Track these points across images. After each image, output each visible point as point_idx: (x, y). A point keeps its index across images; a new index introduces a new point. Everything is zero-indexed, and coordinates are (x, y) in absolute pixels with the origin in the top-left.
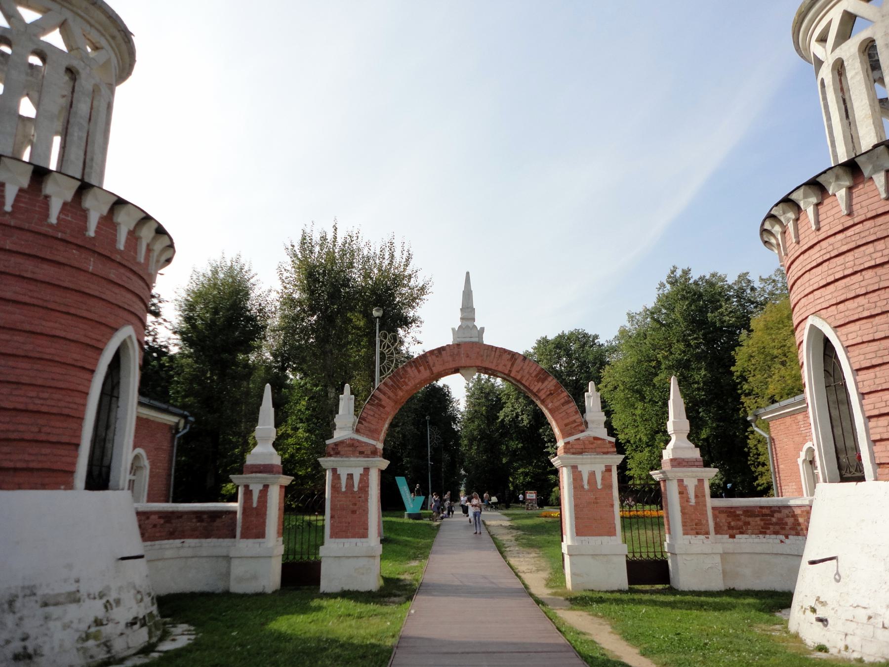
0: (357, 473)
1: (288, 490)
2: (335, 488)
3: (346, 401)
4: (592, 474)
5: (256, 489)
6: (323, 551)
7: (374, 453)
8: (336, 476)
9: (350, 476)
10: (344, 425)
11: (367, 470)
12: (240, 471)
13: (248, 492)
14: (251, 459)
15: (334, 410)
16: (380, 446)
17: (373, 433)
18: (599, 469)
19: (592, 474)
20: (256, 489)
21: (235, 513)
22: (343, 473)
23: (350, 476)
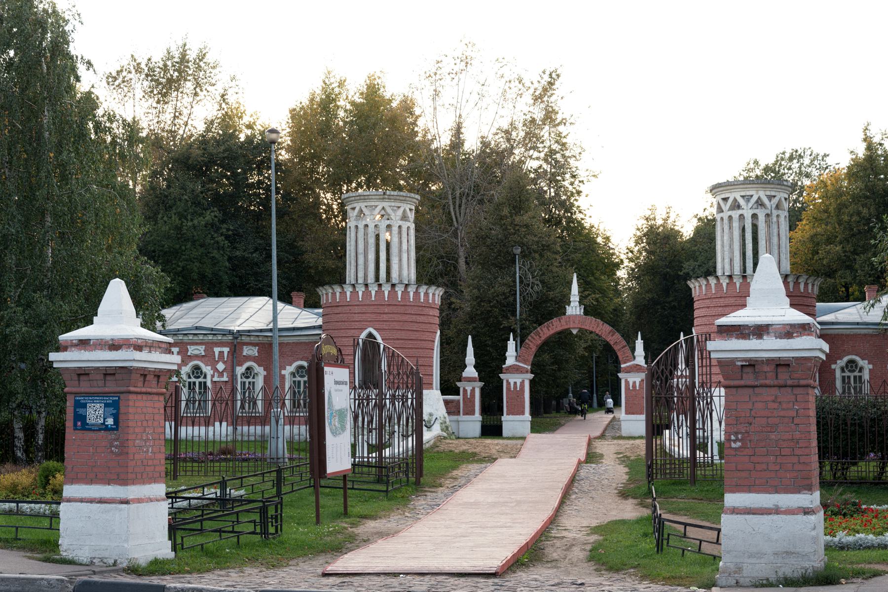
0: (519, 382)
1: (482, 390)
2: (508, 389)
3: (511, 344)
4: (634, 383)
5: (469, 389)
6: (503, 418)
7: (527, 372)
8: (508, 383)
9: (515, 383)
10: (511, 358)
11: (523, 381)
12: (460, 381)
13: (465, 391)
14: (464, 374)
15: (505, 349)
16: (529, 367)
17: (525, 362)
18: (638, 380)
19: (634, 383)
20: (469, 389)
21: (459, 401)
22: (512, 382)
23: (515, 383)
